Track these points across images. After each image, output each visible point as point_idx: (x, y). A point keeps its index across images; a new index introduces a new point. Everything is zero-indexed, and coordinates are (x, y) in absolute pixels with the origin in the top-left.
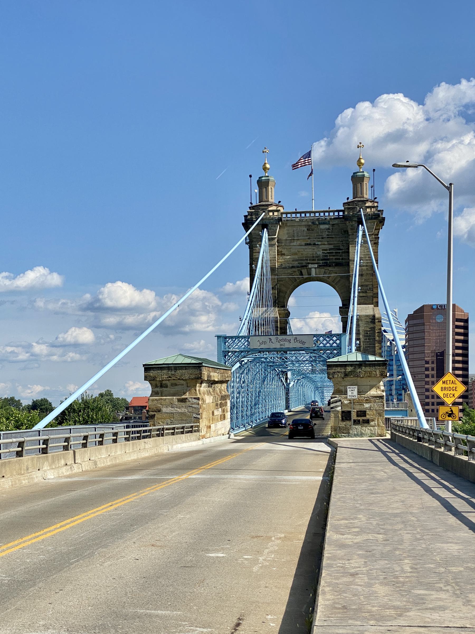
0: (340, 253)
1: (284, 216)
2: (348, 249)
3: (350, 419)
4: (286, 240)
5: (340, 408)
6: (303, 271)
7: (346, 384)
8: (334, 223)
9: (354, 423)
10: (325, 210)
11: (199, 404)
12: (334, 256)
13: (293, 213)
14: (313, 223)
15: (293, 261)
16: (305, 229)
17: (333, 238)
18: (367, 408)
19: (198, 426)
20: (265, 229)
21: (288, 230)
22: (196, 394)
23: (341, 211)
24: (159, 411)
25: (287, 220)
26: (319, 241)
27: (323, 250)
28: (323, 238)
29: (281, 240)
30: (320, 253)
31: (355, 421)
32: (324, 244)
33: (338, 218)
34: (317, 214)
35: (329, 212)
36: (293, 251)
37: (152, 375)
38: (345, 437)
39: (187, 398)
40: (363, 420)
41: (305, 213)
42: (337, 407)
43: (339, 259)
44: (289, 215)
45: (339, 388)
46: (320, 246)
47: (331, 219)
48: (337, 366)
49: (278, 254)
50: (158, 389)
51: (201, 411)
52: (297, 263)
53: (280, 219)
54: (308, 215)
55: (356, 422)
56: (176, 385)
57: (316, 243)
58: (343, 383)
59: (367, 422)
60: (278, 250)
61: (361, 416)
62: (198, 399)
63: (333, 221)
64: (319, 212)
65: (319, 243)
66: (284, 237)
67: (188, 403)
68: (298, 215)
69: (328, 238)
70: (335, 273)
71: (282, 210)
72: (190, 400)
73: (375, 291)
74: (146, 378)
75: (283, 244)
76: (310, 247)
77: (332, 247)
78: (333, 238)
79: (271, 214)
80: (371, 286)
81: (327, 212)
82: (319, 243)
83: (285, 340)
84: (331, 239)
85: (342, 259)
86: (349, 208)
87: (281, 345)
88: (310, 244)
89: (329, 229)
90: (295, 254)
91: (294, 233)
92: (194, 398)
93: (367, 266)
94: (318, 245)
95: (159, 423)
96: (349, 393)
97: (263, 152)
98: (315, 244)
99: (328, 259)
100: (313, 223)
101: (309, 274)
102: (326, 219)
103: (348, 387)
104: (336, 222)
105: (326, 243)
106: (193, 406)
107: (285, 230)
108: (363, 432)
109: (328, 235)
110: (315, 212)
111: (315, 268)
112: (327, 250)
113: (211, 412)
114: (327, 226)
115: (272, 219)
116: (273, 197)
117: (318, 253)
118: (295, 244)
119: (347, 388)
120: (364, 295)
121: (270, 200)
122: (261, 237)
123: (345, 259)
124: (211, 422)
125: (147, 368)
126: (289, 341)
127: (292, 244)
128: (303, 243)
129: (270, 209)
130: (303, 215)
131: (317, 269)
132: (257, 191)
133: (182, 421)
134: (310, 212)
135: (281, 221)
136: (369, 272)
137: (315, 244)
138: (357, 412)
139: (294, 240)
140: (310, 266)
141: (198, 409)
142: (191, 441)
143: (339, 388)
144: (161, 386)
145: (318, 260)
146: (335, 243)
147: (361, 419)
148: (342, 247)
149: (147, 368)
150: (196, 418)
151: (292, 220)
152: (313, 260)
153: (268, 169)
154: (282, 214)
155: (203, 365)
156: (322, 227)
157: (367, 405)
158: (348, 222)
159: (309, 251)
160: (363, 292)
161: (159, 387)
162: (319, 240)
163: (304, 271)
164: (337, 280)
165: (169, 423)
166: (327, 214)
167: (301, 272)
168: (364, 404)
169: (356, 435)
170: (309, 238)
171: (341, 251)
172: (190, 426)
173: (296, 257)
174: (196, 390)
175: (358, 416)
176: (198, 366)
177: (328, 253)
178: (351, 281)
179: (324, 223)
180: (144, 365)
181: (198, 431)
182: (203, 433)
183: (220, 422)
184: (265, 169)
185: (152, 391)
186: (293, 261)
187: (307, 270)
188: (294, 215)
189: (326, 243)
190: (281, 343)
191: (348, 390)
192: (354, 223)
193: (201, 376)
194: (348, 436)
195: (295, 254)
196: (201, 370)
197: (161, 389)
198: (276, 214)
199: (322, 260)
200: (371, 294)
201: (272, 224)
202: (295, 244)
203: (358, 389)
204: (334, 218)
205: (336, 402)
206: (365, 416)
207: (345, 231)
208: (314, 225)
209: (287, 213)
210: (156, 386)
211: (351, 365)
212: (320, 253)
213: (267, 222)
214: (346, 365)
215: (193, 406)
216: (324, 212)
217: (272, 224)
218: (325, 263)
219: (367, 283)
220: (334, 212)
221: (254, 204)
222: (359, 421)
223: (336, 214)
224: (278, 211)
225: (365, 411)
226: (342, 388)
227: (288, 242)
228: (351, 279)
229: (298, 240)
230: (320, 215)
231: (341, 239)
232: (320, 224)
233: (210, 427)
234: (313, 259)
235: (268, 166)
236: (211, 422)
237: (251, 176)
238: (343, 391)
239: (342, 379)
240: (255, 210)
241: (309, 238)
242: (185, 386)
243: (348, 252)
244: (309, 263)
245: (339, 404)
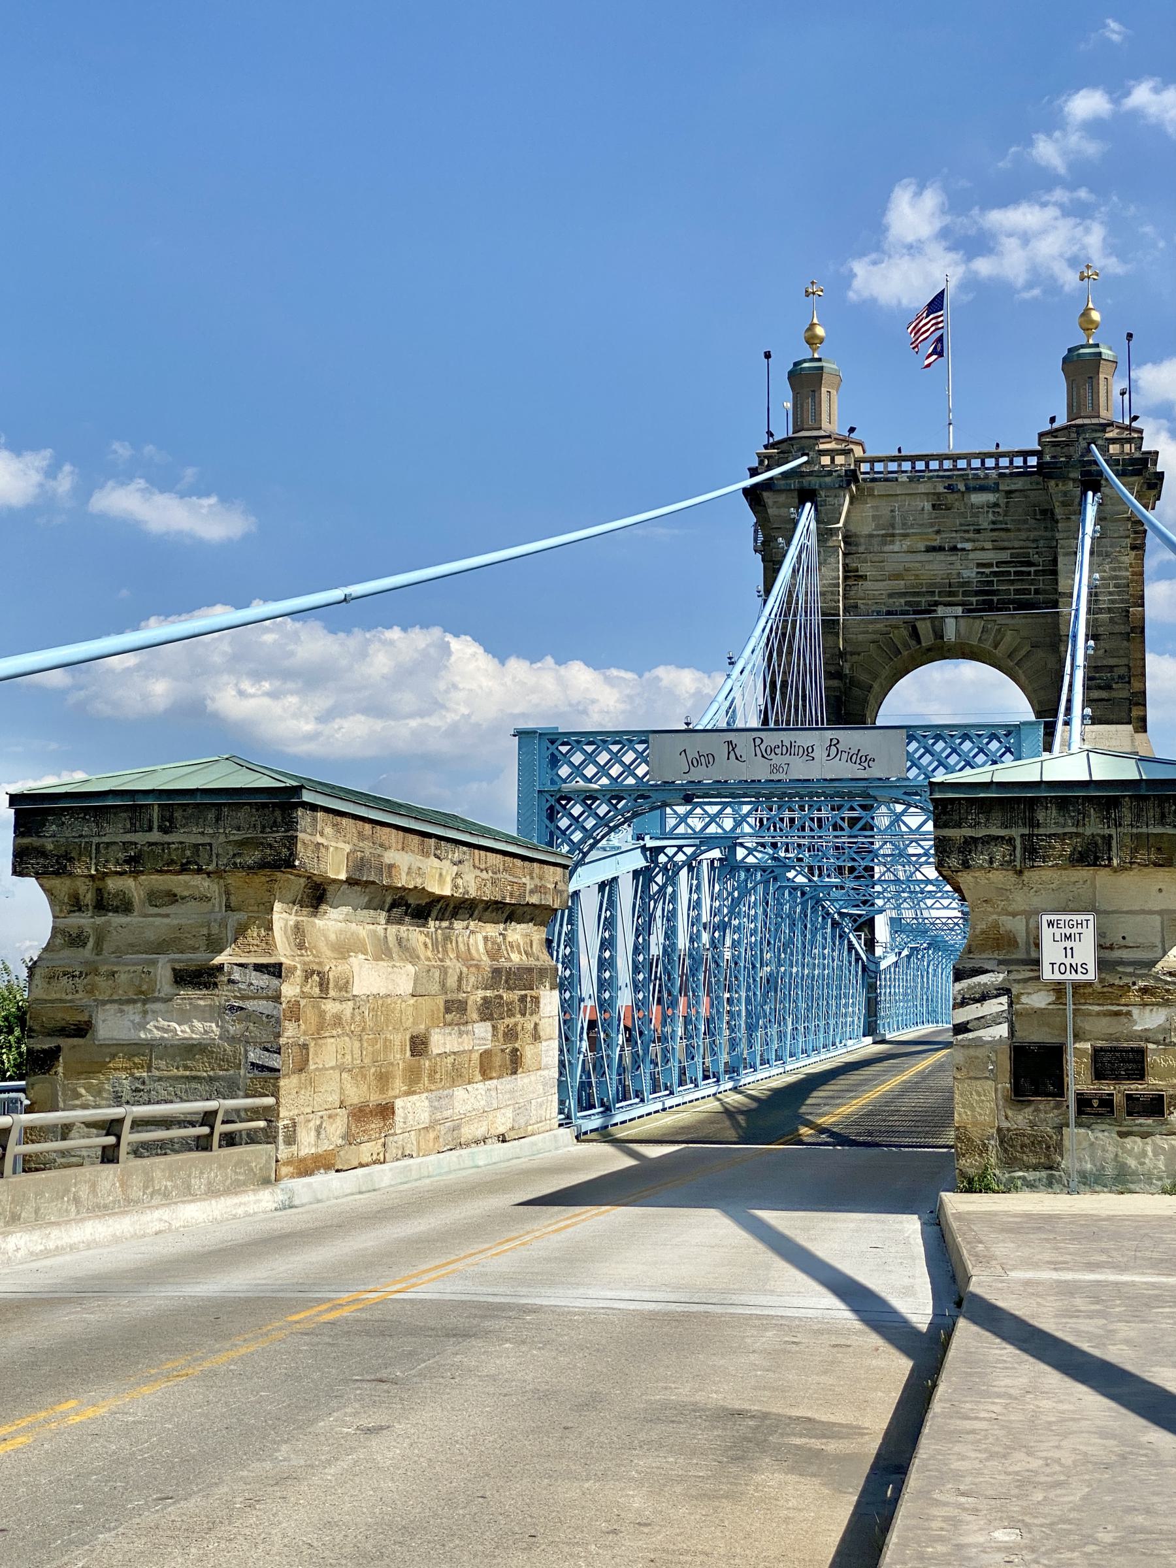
0: (1029, 573)
1: (865, 467)
2: (1055, 562)
3: (1059, 1090)
4: (871, 536)
5: (1002, 1030)
6: (918, 624)
7: (1036, 902)
8: (1013, 487)
9: (1080, 1112)
10: (985, 450)
11: (277, 998)
12: (1012, 582)
13: (893, 459)
14: (949, 487)
15: (890, 596)
16: (928, 506)
17: (1007, 530)
18: (1146, 1036)
19: (269, 1114)
20: (808, 505)
21: (875, 508)
22: (269, 945)
23: (1032, 453)
24: (82, 1030)
25: (873, 480)
26: (968, 540)
27: (979, 565)
28: (978, 531)
29: (856, 535)
30: (970, 573)
31: (1083, 1102)
32: (983, 549)
33: (1025, 473)
34: (962, 464)
35: (997, 456)
36: (890, 567)
37: (50, 847)
38: (1031, 1186)
39: (220, 968)
40: (1129, 1097)
41: (926, 458)
42: (983, 1022)
43: (1028, 592)
44: (879, 467)
45: (996, 925)
46: (971, 556)
47: (1001, 475)
48: (985, 806)
49: (845, 578)
50: (84, 921)
51: (290, 1032)
52: (902, 601)
53: (852, 476)
54: (934, 465)
55: (1092, 1109)
56: (172, 898)
57: (959, 546)
58: (1020, 900)
59: (1155, 1106)
60: (845, 565)
61: (1117, 1078)
62: (275, 970)
63: (1008, 480)
64: (968, 457)
65: (968, 546)
66: (865, 528)
67: (224, 995)
68: (906, 466)
69: (992, 530)
70: (1014, 626)
71: (858, 452)
72: (236, 976)
73: (1136, 685)
74: (22, 863)
75: (861, 549)
76: (940, 556)
77: (1005, 556)
78: (1007, 530)
79: (826, 460)
80: (1122, 671)
81: (990, 455)
82: (968, 546)
83: (790, 750)
84: (1003, 534)
85: (1037, 592)
86: (1055, 444)
87: (775, 768)
88: (941, 549)
89: (996, 505)
90: (897, 576)
91: (894, 517)
92: (259, 968)
93: (1110, 610)
94: (963, 550)
95: (79, 1096)
96: (1051, 953)
97: (807, 294)
98: (954, 549)
99: (993, 593)
100: (949, 487)
101: (939, 634)
102: (987, 476)
103: (1046, 918)
104: (1019, 484)
105: (989, 545)
106: (250, 1005)
107: (867, 509)
108: (1132, 1163)
109: (994, 523)
110: (955, 458)
111: (956, 617)
112: (990, 565)
113: (400, 1039)
114: (990, 497)
115: (830, 473)
116: (835, 417)
117: (966, 573)
118: (896, 548)
119: (1038, 928)
120: (1104, 694)
121: (825, 424)
122: (795, 523)
123: (1045, 592)
124: (399, 1085)
125: (31, 811)
126: (808, 752)
127: (887, 548)
128: (921, 546)
129: (822, 447)
130: (920, 465)
131: (962, 622)
132: (789, 405)
133: (191, 1085)
134: (941, 458)
135: (856, 480)
136: (1118, 629)
137: (954, 549)
138: (1097, 1051)
139: (893, 535)
140: (941, 611)
141: (274, 1024)
142: (188, 1193)
143: (996, 925)
144: (101, 905)
145: (965, 594)
146: (1017, 544)
147: (1117, 1090)
148: (1035, 558)
149: (31, 811)
150: (262, 1068)
151: (887, 480)
152: (951, 594)
153: (822, 340)
154: (858, 461)
155: (307, 797)
156: (977, 498)
157: (1148, 1020)
158: (1052, 483)
159: (937, 568)
160: (1100, 688)
161: (86, 910)
162: (967, 536)
163: (924, 627)
164: (1023, 652)
165: (126, 1096)
166: (990, 462)
167: (914, 628)
168: (1135, 1012)
169: (1091, 1181)
170: (938, 532)
171: (1032, 569)
172: (228, 1105)
173: (900, 585)
174: (269, 928)
175: (1099, 1074)
176: (280, 806)
177: (995, 574)
178: (1063, 654)
179: (982, 489)
180: (14, 799)
181: (268, 1136)
182: (307, 1144)
183: (480, 1087)
184: (812, 340)
185: (55, 930)
186: (890, 596)
187: (932, 623)
188: (893, 466)
189: (989, 545)
190: (776, 760)
191: (1047, 933)
192: (1071, 484)
193: (293, 855)
194: (1050, 1184)
195: (897, 576)
196: (291, 824)
197: (99, 920)
198: (840, 460)
199: (977, 593)
200: (1125, 694)
201: (828, 488)
202: (896, 548)
203: (1100, 934)
204: (1012, 474)
205: (983, 998)
206: (1139, 1074)
207: (1044, 512)
208: (951, 485)
209: (872, 461)
210: (76, 905)
211: (1063, 804)
212: (970, 573)
213: (814, 482)
214: (1032, 803)
215: (250, 1005)
216: (983, 456)
217: (828, 488)
218: (985, 600)
219: (1112, 662)
220: (1011, 455)
221: (777, 438)
222: (1107, 1103)
223: (1019, 461)
224: (847, 452)
225: (1141, 1053)
226: (1017, 926)
227: (875, 541)
228: (1063, 649)
229: (905, 535)
230: (969, 464)
231: (1032, 535)
232: (969, 489)
233: (386, 1111)
234: (950, 592)
235: (820, 331)
236: (399, 1085)
237: (768, 355)
238: (1021, 938)
239: (1011, 877)
240: (781, 450)
241: (938, 532)
242: (218, 901)
243: (1055, 573)
244: (936, 604)
245: (997, 1005)
